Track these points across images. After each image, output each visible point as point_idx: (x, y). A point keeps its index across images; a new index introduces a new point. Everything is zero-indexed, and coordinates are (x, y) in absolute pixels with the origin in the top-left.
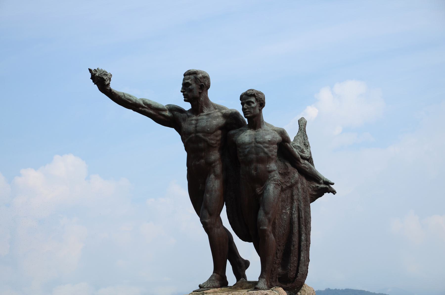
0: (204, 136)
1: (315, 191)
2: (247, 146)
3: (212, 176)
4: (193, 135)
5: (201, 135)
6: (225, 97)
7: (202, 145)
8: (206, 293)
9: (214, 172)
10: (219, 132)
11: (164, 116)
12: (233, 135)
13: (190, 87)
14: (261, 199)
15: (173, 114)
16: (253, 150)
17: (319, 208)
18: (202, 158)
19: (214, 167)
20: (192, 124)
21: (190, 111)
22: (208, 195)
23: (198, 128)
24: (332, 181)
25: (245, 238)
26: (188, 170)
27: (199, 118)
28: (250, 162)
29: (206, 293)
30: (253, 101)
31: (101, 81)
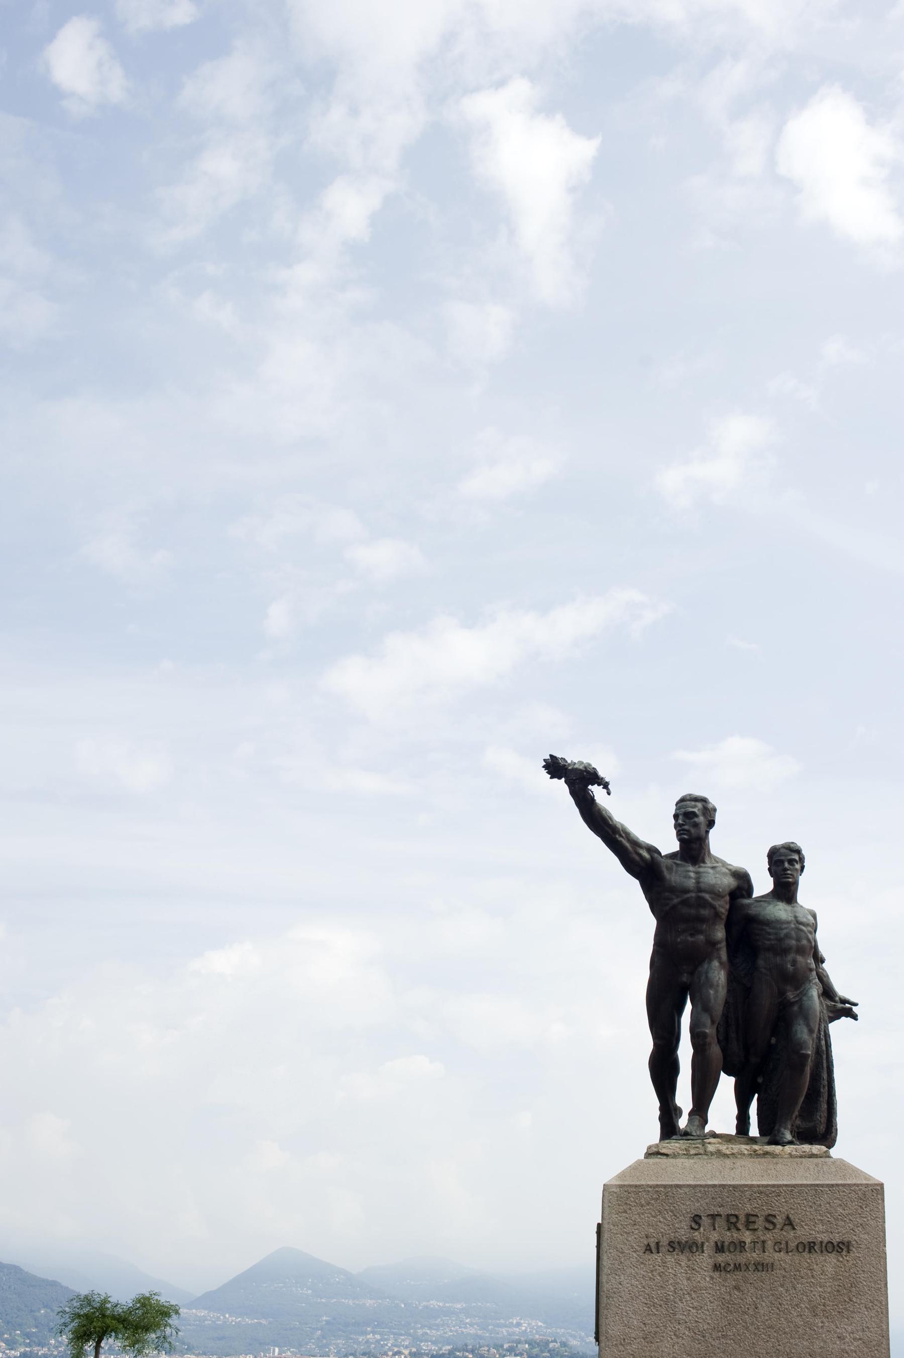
0: (712, 898)
1: (831, 1011)
2: (784, 926)
3: (716, 963)
4: (693, 895)
5: (707, 896)
7: (705, 912)
8: (709, 1143)
9: (719, 958)
10: (728, 898)
11: (640, 855)
13: (696, 820)
14: (796, 1008)
15: (652, 857)
16: (793, 933)
18: (700, 932)
19: (718, 950)
20: (690, 877)
21: (673, 856)
22: (712, 992)
23: (702, 885)
27: (701, 870)
28: (786, 951)
29: (709, 1143)
30: (785, 863)
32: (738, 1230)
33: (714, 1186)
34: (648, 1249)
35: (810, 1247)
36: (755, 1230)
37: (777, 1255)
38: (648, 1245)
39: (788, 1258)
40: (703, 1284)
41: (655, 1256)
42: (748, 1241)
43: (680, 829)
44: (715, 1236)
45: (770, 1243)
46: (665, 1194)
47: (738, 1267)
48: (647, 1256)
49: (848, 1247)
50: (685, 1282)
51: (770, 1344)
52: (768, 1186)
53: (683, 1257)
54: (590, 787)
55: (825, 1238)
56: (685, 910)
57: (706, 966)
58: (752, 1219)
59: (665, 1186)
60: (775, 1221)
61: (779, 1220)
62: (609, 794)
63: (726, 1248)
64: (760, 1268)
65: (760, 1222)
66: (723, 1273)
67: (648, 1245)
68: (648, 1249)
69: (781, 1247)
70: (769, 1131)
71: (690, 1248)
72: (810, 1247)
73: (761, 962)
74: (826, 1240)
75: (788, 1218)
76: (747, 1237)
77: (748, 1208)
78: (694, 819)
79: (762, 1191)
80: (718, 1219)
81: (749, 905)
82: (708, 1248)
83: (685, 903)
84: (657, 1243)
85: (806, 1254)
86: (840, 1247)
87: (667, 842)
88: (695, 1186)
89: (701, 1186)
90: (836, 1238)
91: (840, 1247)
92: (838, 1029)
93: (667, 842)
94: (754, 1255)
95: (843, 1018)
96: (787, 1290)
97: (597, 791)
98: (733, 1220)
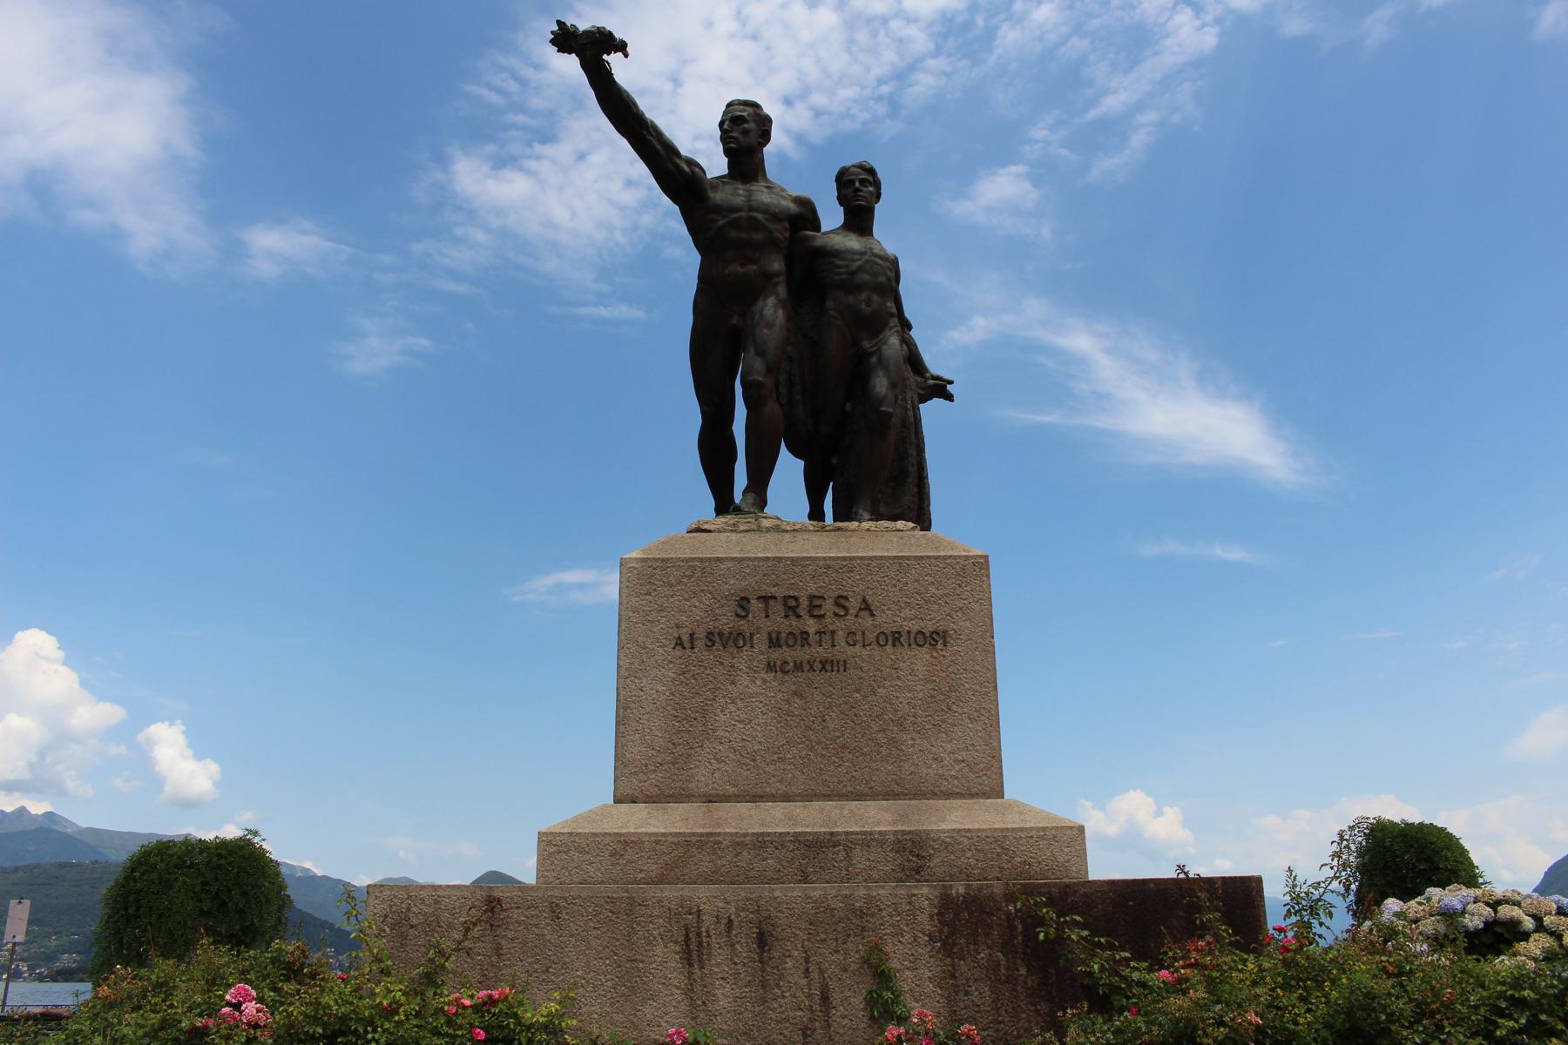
3: (771, 301)
5: (760, 216)
11: (677, 166)
14: (874, 360)
24: (947, 376)
31: (593, 48)
32: (799, 617)
33: (767, 559)
35: (896, 638)
36: (822, 616)
37: (850, 650)
39: (865, 652)
40: (753, 689)
42: (812, 631)
43: (726, 138)
44: (766, 626)
46: (699, 570)
47: (798, 667)
48: (678, 652)
51: (843, 770)
54: (605, 57)
55: (914, 626)
56: (733, 234)
57: (760, 303)
58: (817, 602)
59: (701, 560)
61: (854, 604)
62: (626, 56)
64: (828, 667)
65: (828, 607)
66: (779, 674)
68: (679, 643)
70: (842, 514)
73: (830, 304)
74: (915, 629)
75: (864, 600)
76: (811, 626)
77: (812, 588)
78: (745, 130)
79: (828, 565)
80: (772, 603)
81: (813, 237)
82: (761, 642)
83: (733, 224)
85: (889, 648)
86: (934, 639)
87: (715, 163)
88: (742, 559)
90: (929, 627)
91: (934, 639)
92: (931, 412)
93: (715, 163)
94: (821, 650)
96: (865, 697)
97: (614, 60)
98: (792, 603)
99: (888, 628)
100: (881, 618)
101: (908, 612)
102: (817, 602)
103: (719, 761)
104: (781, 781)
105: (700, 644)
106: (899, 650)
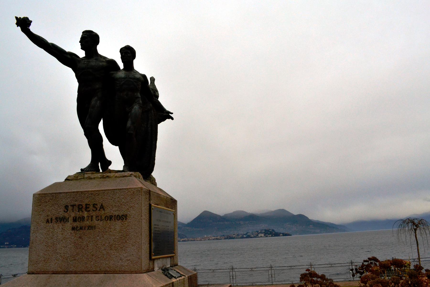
3: (96, 98)
6: (109, 49)
12: (113, 74)
14: (130, 114)
17: (163, 128)
24: (171, 112)
25: (113, 142)
26: (78, 95)
27: (91, 60)
30: (128, 53)
31: (24, 24)
32: (82, 211)
33: (74, 192)
34: (48, 221)
35: (110, 218)
36: (89, 211)
38: (48, 220)
39: (101, 223)
41: (50, 224)
42: (86, 216)
44: (73, 215)
45: (94, 217)
47: (81, 228)
49: (126, 217)
50: (61, 236)
51: (92, 263)
52: (95, 191)
53: (61, 225)
55: (116, 213)
58: (88, 206)
60: (97, 207)
61: (99, 206)
63: (77, 220)
64: (90, 228)
65: (91, 207)
66: (76, 231)
67: (48, 220)
68: (48, 221)
69: (99, 218)
71: (64, 220)
72: (110, 218)
74: (117, 214)
75: (102, 205)
76: (86, 214)
77: (87, 201)
78: (90, 40)
80: (75, 207)
84: (51, 219)
85: (108, 221)
86: (123, 217)
89: (69, 192)
90: (121, 213)
91: (123, 217)
94: (88, 222)
95: (167, 120)
99: (108, 215)
100: (106, 212)
101: (115, 209)
102: (88, 206)
103: (57, 260)
104: (74, 267)
105: (53, 221)
106: (112, 221)
